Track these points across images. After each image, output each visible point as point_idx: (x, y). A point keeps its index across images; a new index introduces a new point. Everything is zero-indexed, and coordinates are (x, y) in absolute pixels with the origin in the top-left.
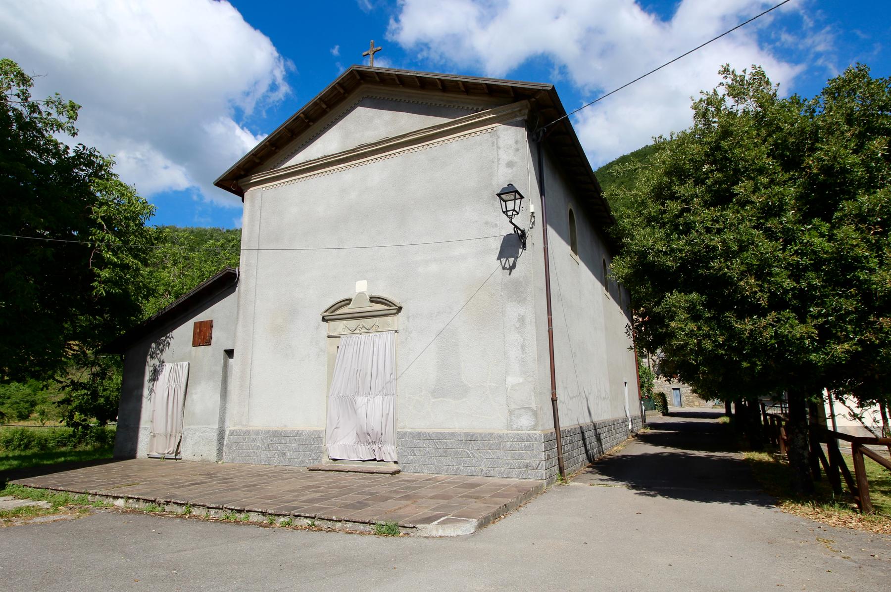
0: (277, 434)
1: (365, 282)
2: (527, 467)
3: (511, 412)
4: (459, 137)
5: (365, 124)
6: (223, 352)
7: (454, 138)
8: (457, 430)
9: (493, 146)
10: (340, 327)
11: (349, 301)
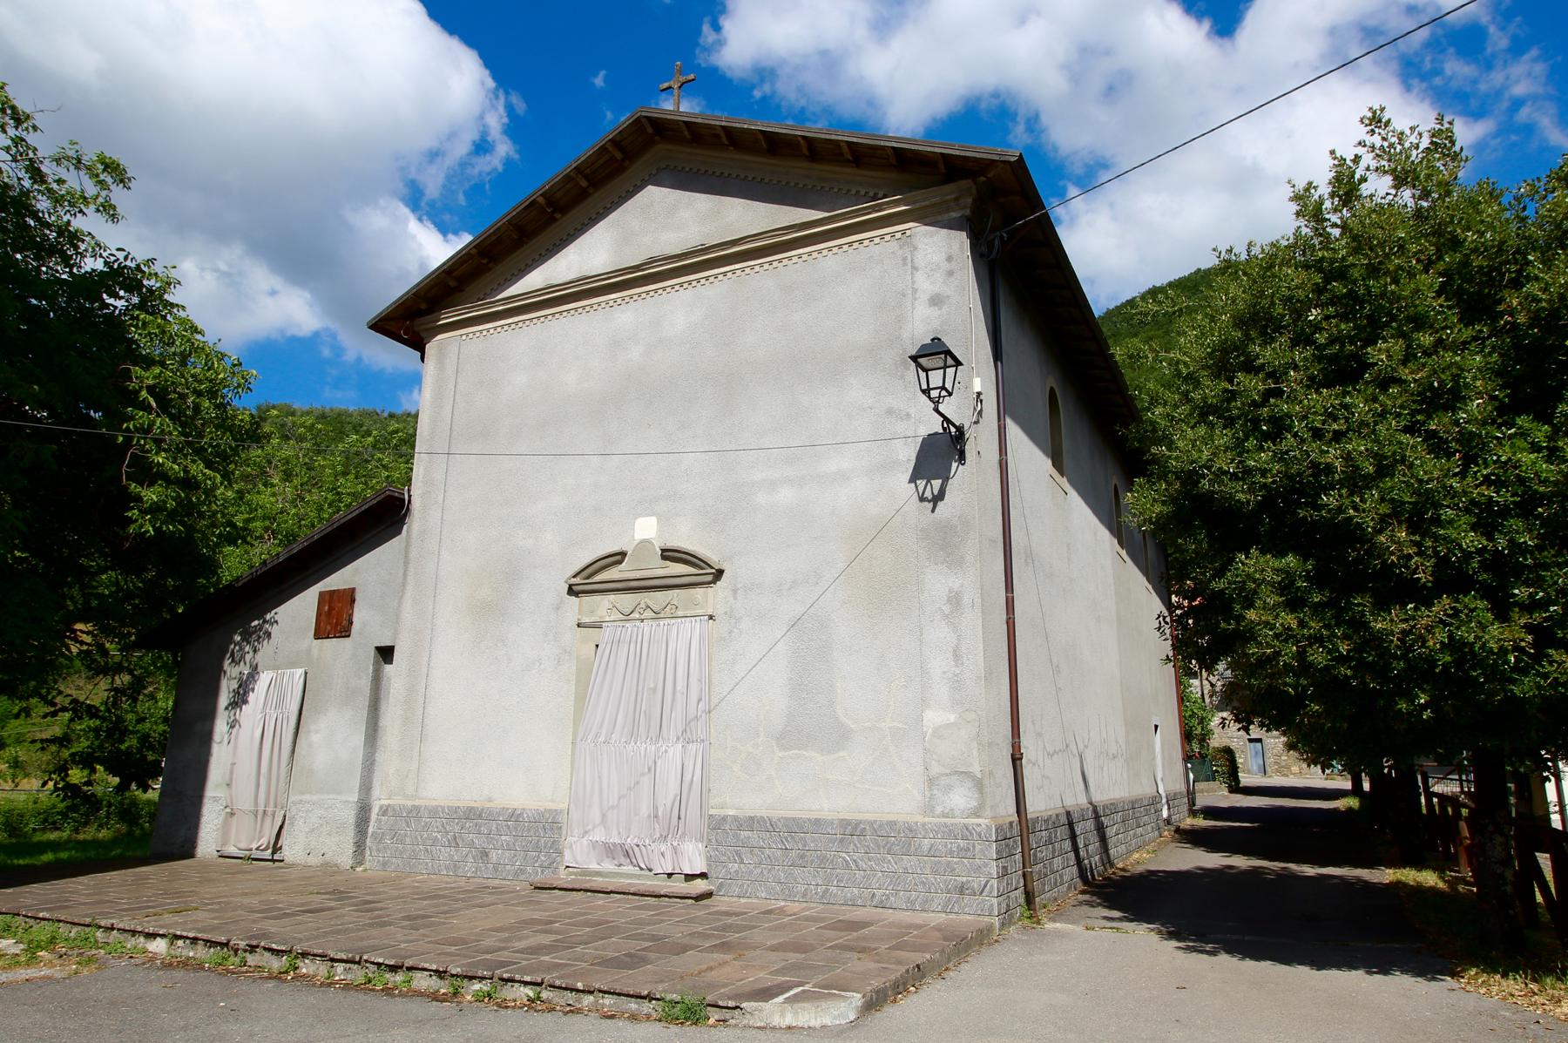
0: (473, 815)
1: (653, 520)
2: (962, 890)
3: (931, 781)
4: (840, 247)
5: (661, 218)
6: (372, 652)
7: (830, 249)
8: (825, 815)
9: (905, 264)
10: (602, 605)
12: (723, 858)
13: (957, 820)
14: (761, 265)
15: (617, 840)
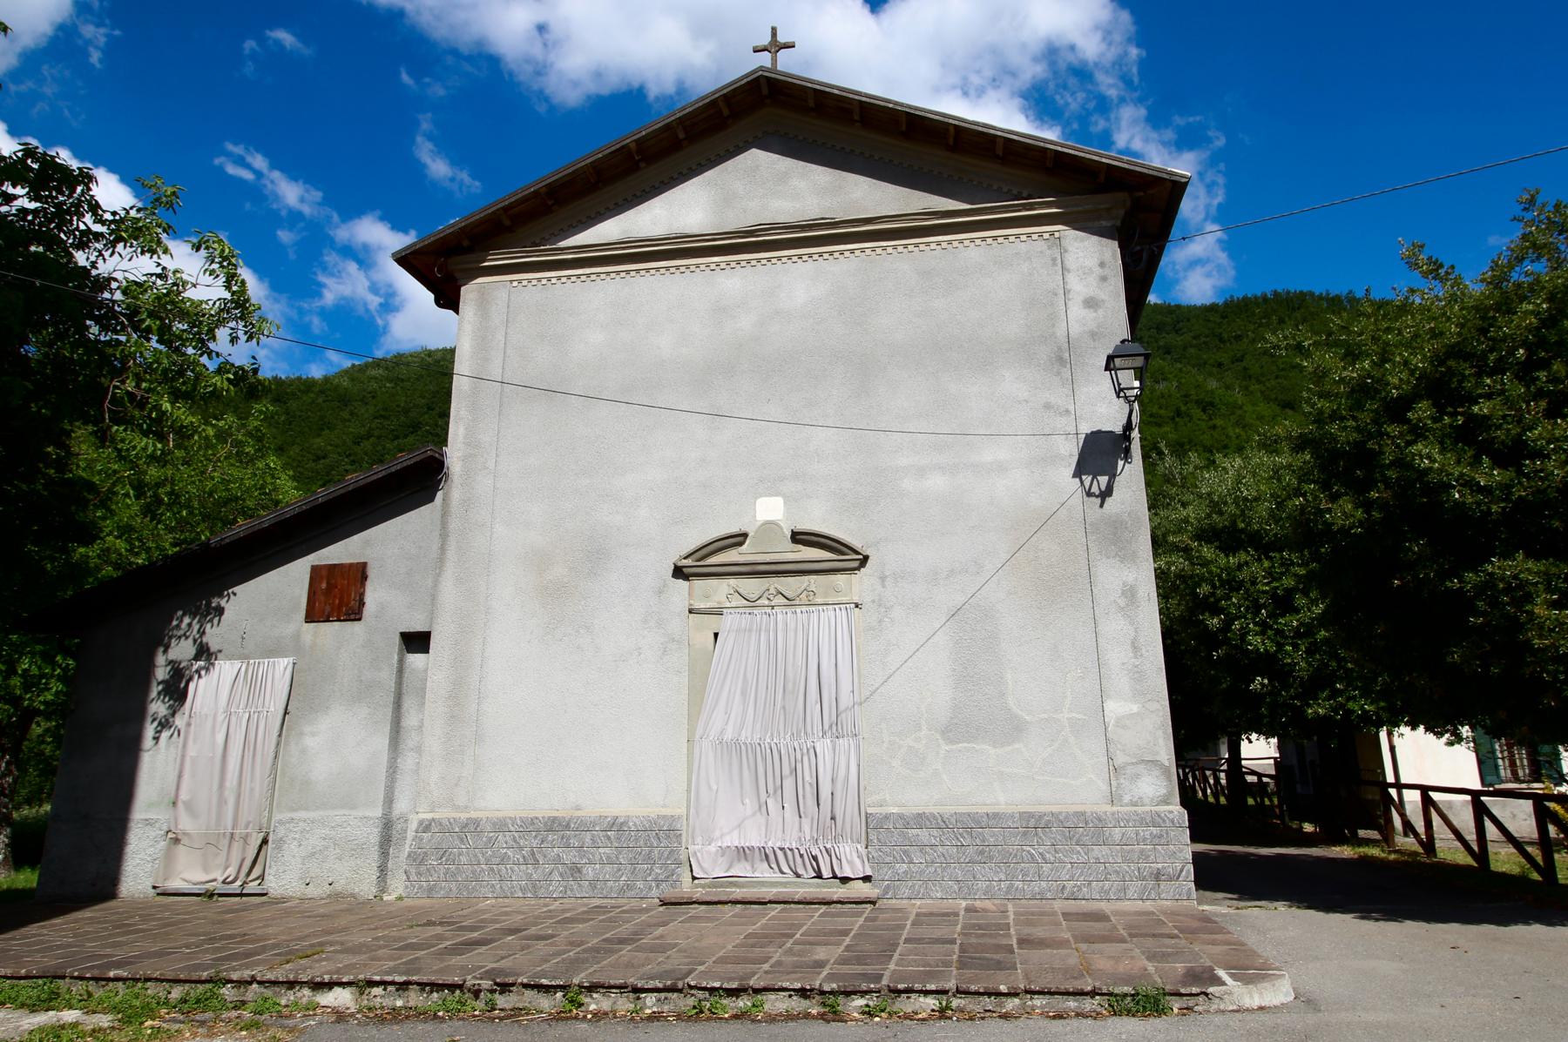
0: (555, 826)
1: (779, 501)
2: (1157, 876)
4: (984, 239)
5: (765, 184)
6: (397, 639)
8: (1001, 808)
9: (1054, 264)
10: (718, 591)
11: (739, 539)
12: (888, 859)
13: (1147, 808)
14: (895, 247)
15: (755, 844)
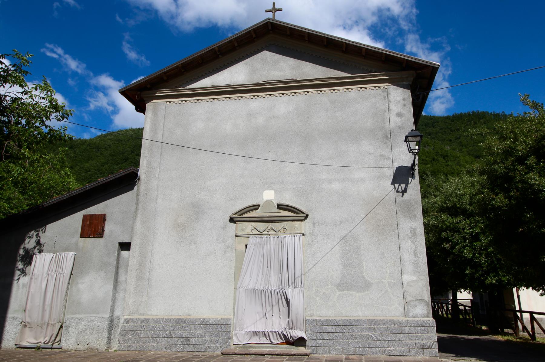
0: (179, 322)
1: (273, 192)
2: (423, 347)
3: (407, 303)
4: (357, 88)
5: (270, 65)
6: (117, 245)
7: (352, 89)
8: (360, 318)
10: (248, 228)
11: (256, 207)
12: (314, 338)
13: (419, 319)
14: (321, 91)
15: (261, 330)
